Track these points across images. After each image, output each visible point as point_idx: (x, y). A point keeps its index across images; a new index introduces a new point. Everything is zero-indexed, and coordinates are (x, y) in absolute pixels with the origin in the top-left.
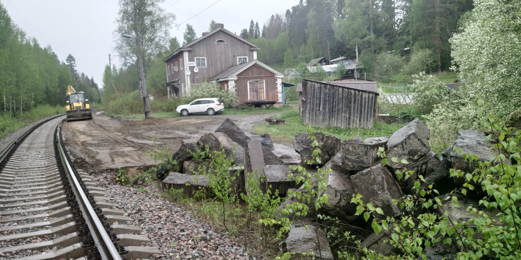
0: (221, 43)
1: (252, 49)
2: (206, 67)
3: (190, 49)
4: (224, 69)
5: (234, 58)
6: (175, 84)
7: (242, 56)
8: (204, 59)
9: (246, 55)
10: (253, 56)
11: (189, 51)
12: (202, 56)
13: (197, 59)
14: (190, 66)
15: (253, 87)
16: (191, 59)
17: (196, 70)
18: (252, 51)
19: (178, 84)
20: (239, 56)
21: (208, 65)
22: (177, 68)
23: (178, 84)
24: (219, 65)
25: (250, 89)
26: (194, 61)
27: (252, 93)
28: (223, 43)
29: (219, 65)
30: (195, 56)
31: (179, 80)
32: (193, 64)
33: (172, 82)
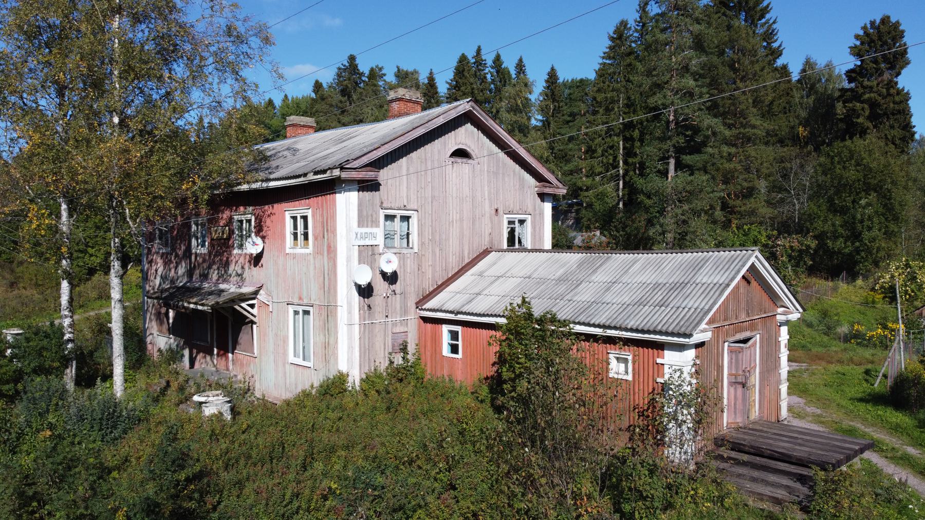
0: (465, 160)
1: (548, 190)
4: (467, 261)
5: (496, 218)
6: (244, 305)
10: (542, 214)
14: (362, 243)
15: (737, 369)
16: (365, 219)
19: (252, 306)
20: (509, 213)
21: (422, 244)
24: (453, 246)
25: (730, 375)
26: (375, 223)
27: (732, 390)
29: (453, 246)
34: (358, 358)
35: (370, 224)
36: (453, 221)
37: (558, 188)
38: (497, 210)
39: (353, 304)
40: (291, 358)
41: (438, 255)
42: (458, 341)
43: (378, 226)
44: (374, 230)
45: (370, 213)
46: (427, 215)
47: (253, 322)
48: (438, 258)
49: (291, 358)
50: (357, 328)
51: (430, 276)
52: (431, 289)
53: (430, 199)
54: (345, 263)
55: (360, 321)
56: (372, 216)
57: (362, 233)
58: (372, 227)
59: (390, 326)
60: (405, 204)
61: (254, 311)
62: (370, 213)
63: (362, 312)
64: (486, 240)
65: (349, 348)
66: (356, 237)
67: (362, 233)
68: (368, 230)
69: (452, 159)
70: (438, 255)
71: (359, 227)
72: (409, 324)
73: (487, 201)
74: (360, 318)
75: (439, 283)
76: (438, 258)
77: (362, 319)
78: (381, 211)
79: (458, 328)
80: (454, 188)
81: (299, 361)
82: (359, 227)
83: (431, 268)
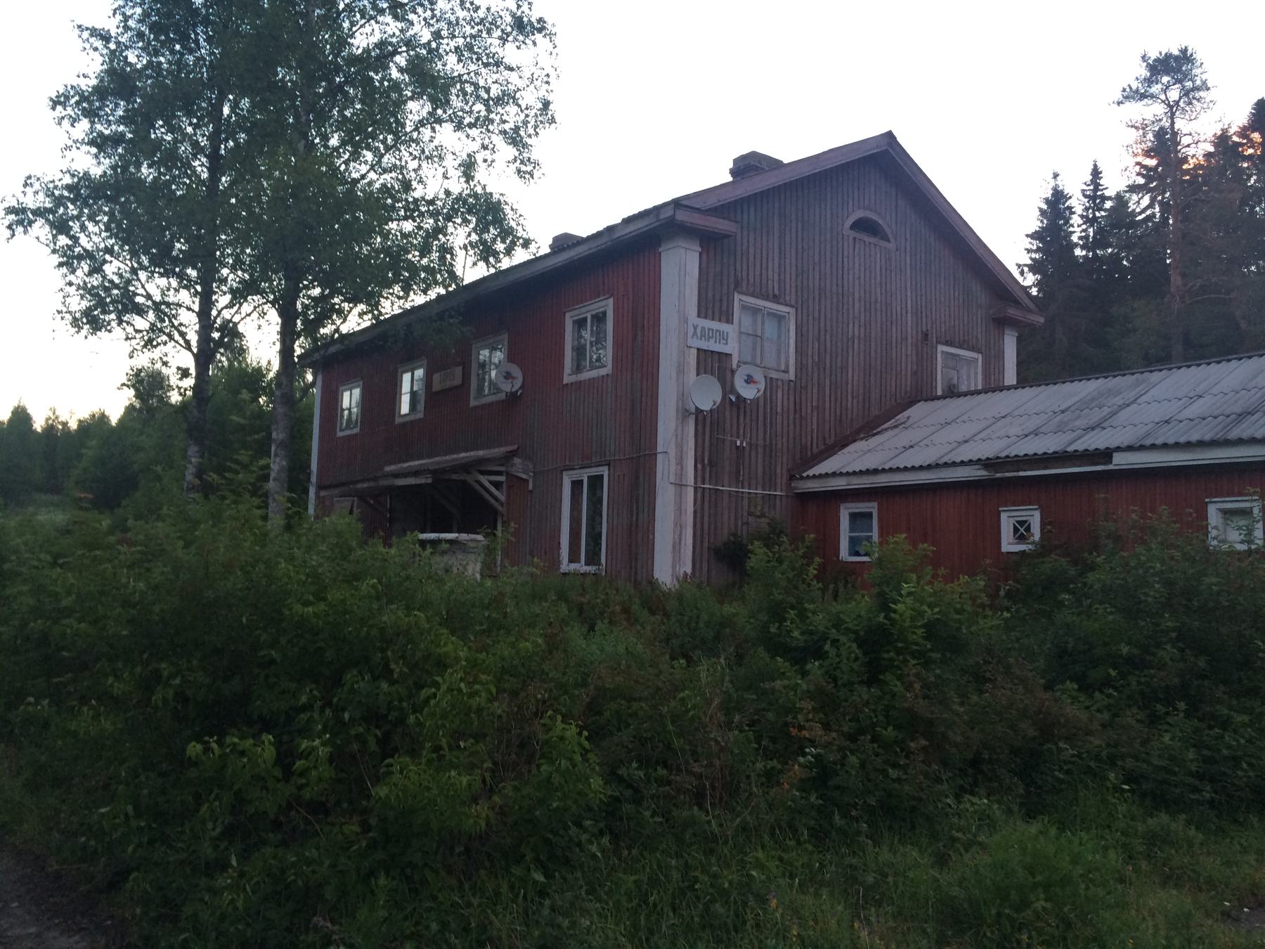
0: (872, 240)
2: (792, 377)
3: (722, 225)
6: (484, 480)
7: (960, 347)
8: (780, 318)
9: (972, 349)
10: (1000, 356)
11: (710, 242)
12: (775, 299)
13: (744, 307)
14: (704, 345)
17: (749, 380)
18: (1001, 323)
19: (497, 485)
21: (801, 367)
22: (516, 372)
23: (497, 485)
28: (883, 243)
30: (737, 285)
31: (513, 454)
32: (724, 338)
33: (467, 467)
34: (691, 548)
35: (717, 316)
36: (853, 337)
37: (1030, 311)
38: (926, 336)
39: (685, 450)
40: (566, 566)
41: (827, 392)
42: (871, 531)
43: (729, 320)
44: (724, 327)
45: (718, 298)
46: (811, 318)
47: (495, 512)
48: (827, 399)
49: (566, 566)
50: (690, 492)
51: (815, 427)
52: (815, 450)
53: (817, 292)
54: (674, 375)
55: (695, 483)
56: (721, 300)
57: (703, 328)
58: (720, 321)
59: (746, 502)
60: (776, 292)
61: (503, 498)
62: (718, 298)
63: (699, 466)
64: (909, 383)
65: (675, 525)
66: (695, 333)
67: (703, 328)
68: (715, 325)
69: (853, 234)
70: (827, 392)
71: (699, 316)
72: (778, 501)
73: (909, 315)
74: (696, 478)
75: (830, 442)
76: (827, 399)
77: (699, 479)
78: (736, 294)
79: (872, 507)
80: (857, 282)
81: (582, 567)
82: (699, 316)
83: (815, 413)
